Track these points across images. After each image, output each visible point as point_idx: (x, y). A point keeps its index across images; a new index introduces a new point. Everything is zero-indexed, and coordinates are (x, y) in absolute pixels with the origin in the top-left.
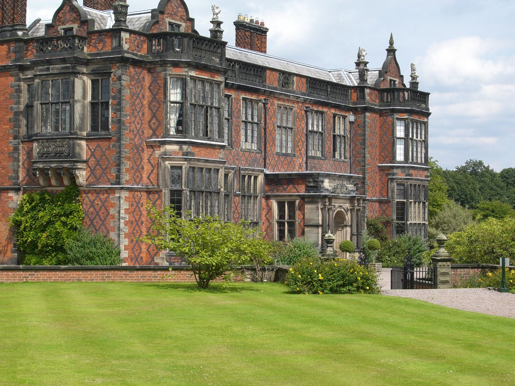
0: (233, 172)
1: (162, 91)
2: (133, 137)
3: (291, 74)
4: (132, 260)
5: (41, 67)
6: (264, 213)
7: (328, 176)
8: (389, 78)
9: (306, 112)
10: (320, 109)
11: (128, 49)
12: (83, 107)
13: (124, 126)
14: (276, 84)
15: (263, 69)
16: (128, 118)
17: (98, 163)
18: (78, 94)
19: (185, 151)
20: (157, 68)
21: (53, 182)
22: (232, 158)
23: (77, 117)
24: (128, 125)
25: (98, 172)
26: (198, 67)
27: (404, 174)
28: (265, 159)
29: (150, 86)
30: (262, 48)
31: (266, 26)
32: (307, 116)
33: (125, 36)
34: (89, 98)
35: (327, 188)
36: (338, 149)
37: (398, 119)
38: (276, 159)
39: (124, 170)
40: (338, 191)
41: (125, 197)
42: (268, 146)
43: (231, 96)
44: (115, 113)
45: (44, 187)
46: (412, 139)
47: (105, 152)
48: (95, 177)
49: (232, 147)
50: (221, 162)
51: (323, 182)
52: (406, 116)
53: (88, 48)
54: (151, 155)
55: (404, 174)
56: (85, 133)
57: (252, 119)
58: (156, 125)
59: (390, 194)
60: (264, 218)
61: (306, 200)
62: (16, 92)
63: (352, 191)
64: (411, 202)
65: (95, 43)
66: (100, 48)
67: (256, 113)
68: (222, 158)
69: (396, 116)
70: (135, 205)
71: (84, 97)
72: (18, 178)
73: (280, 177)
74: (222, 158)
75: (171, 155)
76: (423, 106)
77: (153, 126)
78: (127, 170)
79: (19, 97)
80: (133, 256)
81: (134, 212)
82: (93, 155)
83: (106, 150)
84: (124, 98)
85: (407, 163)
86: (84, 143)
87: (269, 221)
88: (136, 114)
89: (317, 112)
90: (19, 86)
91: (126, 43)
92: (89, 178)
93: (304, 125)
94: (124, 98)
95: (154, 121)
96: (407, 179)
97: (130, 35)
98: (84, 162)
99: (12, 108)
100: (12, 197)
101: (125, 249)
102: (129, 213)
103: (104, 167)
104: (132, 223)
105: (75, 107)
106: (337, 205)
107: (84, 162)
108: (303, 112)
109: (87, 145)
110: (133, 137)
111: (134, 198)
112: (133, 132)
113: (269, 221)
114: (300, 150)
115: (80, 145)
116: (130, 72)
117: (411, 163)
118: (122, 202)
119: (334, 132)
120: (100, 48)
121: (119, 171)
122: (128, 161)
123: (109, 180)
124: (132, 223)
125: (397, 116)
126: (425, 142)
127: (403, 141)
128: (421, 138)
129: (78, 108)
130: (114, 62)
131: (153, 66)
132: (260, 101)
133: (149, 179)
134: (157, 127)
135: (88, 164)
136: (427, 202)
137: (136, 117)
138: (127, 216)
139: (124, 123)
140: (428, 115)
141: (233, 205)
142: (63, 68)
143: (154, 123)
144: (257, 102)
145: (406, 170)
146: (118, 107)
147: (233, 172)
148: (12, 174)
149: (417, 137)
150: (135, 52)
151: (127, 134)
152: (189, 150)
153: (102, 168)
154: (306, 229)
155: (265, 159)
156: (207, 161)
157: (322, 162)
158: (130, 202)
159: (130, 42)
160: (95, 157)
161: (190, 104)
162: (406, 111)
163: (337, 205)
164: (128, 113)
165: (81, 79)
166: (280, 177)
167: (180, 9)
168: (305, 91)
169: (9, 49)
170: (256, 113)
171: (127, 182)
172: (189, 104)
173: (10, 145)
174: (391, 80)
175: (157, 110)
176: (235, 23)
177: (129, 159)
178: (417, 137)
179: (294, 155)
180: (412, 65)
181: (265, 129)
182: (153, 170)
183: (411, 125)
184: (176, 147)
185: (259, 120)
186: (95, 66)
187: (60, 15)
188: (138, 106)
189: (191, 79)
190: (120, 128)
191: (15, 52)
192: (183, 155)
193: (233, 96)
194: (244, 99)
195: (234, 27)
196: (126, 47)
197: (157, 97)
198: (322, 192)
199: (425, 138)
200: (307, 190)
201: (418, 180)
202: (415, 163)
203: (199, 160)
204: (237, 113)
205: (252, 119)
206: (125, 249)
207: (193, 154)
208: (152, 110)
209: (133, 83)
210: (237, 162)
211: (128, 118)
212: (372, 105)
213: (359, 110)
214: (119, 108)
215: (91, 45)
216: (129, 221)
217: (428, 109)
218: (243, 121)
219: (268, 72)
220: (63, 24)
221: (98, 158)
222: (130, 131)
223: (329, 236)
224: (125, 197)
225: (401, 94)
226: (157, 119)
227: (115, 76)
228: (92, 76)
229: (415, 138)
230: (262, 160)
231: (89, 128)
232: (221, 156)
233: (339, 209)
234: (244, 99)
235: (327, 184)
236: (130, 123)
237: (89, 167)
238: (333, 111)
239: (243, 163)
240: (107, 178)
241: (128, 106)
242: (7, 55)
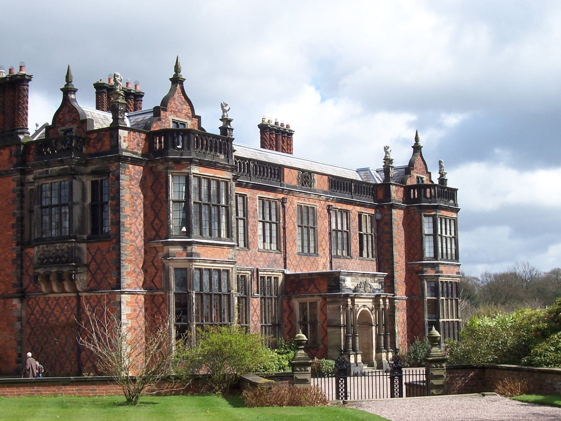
1: (164, 190)
2: (134, 238)
3: (310, 173)
5: (40, 170)
6: (286, 314)
7: (350, 274)
8: (416, 175)
9: (329, 211)
10: (345, 207)
11: (127, 147)
12: (83, 209)
13: (124, 227)
14: (295, 183)
15: (280, 168)
16: (128, 219)
17: (99, 268)
18: (77, 197)
19: (189, 252)
20: (159, 167)
21: (55, 289)
22: (248, 258)
23: (76, 219)
24: (128, 226)
25: (99, 277)
28: (285, 259)
29: (152, 186)
30: (288, 149)
31: (291, 128)
32: (329, 214)
33: (123, 133)
34: (89, 200)
35: (349, 287)
36: (365, 248)
37: (425, 216)
38: (298, 259)
39: (125, 274)
40: (362, 289)
41: (127, 301)
42: (288, 245)
43: (246, 195)
44: (114, 214)
45: (46, 294)
46: (441, 236)
47: (105, 255)
48: (96, 282)
49: (248, 248)
50: (230, 263)
51: (344, 281)
53: (87, 148)
54: (154, 257)
56: (85, 237)
57: (270, 219)
58: (159, 226)
60: (285, 319)
61: (328, 300)
62: (18, 197)
63: (377, 289)
64: (443, 300)
65: (94, 143)
66: (98, 148)
67: (273, 212)
68: (232, 259)
71: (84, 198)
72: (22, 285)
73: (301, 278)
74: (232, 259)
75: (174, 257)
76: (452, 201)
77: (156, 227)
78: (128, 273)
79: (22, 202)
81: (137, 317)
82: (93, 258)
83: (107, 252)
84: (123, 198)
85: (437, 259)
86: (84, 246)
87: (291, 323)
88: (137, 214)
89: (341, 210)
90: (22, 191)
91: (124, 141)
92: (90, 282)
93: (327, 224)
94: (123, 198)
95: (157, 221)
97: (129, 133)
98: (85, 265)
99: (14, 214)
100: (15, 305)
102: (131, 319)
103: (104, 271)
105: (74, 210)
106: (360, 305)
107: (85, 265)
109: (88, 249)
110: (134, 238)
111: (137, 303)
112: (134, 233)
113: (291, 323)
114: (324, 250)
115: (79, 249)
116: (130, 172)
117: (441, 260)
118: (123, 307)
119: (360, 229)
120: (98, 148)
121: (119, 274)
122: (129, 264)
123: (109, 284)
126: (456, 239)
127: (431, 238)
128: (451, 234)
129: (77, 210)
130: (112, 161)
131: (154, 165)
133: (152, 281)
134: (160, 228)
135: (89, 269)
137: (137, 218)
138: (130, 322)
139: (124, 225)
140: (457, 211)
141: (251, 308)
142: (61, 170)
143: (157, 224)
146: (117, 208)
148: (15, 281)
149: (446, 234)
150: (136, 151)
151: (128, 235)
153: (103, 272)
154: (329, 330)
155: (285, 259)
156: (214, 262)
157: (347, 261)
158: (132, 307)
159: (128, 140)
160: (95, 261)
161: (194, 203)
163: (360, 305)
164: (128, 213)
165: (80, 180)
166: (301, 278)
167: (185, 106)
169: (11, 153)
170: (273, 212)
171: (129, 286)
172: (192, 203)
173: (14, 252)
174: (418, 178)
175: (160, 210)
176: (260, 126)
177: (130, 261)
178: (446, 234)
180: (440, 162)
181: (284, 229)
182: (157, 273)
183: (439, 222)
184: (179, 249)
185: (278, 219)
186: (94, 167)
187: (60, 116)
188: (139, 206)
189: (194, 176)
190: (119, 230)
191: (16, 156)
192: (187, 256)
193: (248, 196)
194: (260, 198)
195: (259, 130)
196: (124, 145)
197: (159, 196)
198: (344, 291)
199: (455, 235)
200: (328, 289)
201: (449, 276)
202: (445, 260)
203: (205, 261)
204: (254, 212)
205: (270, 219)
208: (154, 210)
209: (133, 183)
210: (254, 263)
211: (128, 219)
213: (386, 207)
214: (117, 209)
215: (89, 146)
216: (132, 327)
217: (456, 205)
218: (260, 221)
220: (63, 125)
221: (99, 262)
223: (299, 337)
224: (127, 301)
225: (428, 190)
226: (160, 220)
227: (114, 176)
228: (91, 177)
229: (444, 234)
230: (282, 260)
231: (89, 231)
232: (230, 256)
233: (362, 309)
234: (260, 198)
235: (349, 283)
236: (131, 224)
237: (90, 271)
238: (358, 209)
239: (261, 263)
240: (108, 282)
242: (9, 159)
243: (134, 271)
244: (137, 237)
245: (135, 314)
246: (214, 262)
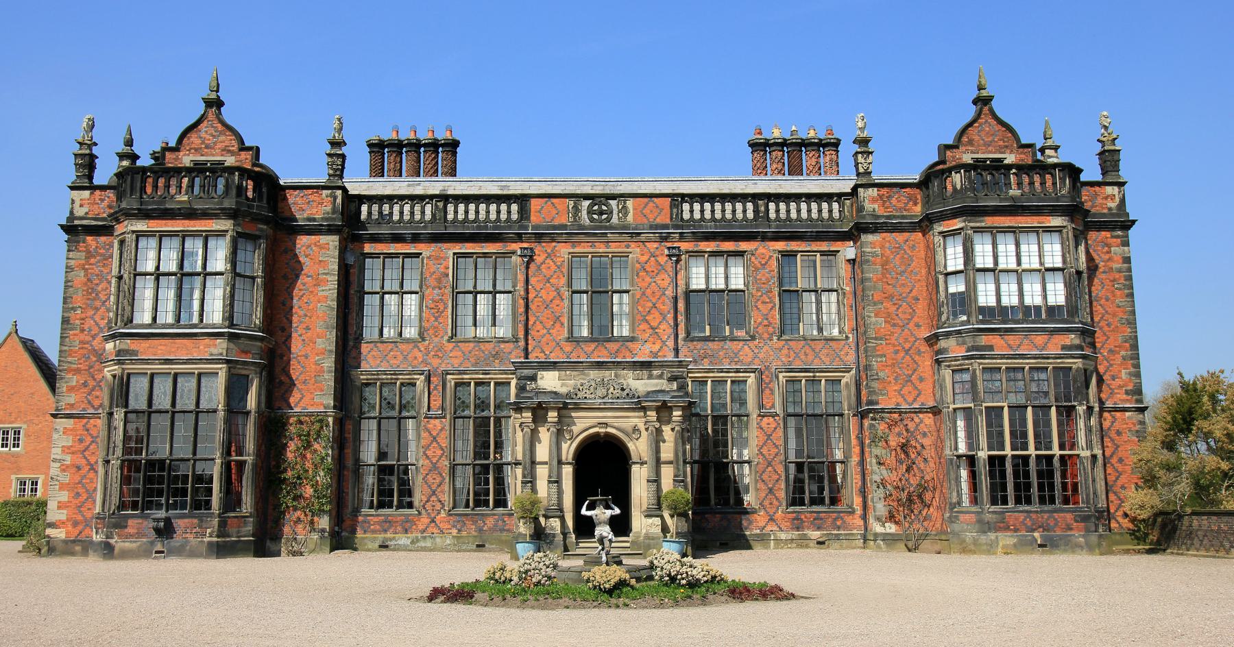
0: (422, 377)
4: (75, 524)
16: (79, 312)
24: (78, 322)
26: (145, 215)
27: (964, 348)
52: (958, 224)
55: (964, 348)
59: (938, 396)
69: (939, 228)
70: (89, 439)
80: (80, 518)
96: (968, 358)
101: (59, 508)
104: (79, 468)
108: (663, 260)
110: (88, 338)
124: (79, 468)
125: (941, 229)
132: (514, 253)
136: (1081, 404)
137: (97, 309)
144: (507, 255)
145: (967, 339)
147: (422, 377)
152: (123, 347)
156: (168, 361)
162: (955, 214)
168: (668, 221)
171: (72, 406)
177: (77, 371)
179: (632, 339)
180: (1047, 122)
193: (426, 254)
203: (146, 361)
206: (59, 508)
207: (135, 353)
209: (92, 260)
212: (888, 217)
219: (533, 201)
222: (83, 330)
232: (215, 351)
238: (781, 245)
241: (80, 294)
243: (85, 385)
244: (94, 337)
245: (82, 447)
246: (168, 361)
